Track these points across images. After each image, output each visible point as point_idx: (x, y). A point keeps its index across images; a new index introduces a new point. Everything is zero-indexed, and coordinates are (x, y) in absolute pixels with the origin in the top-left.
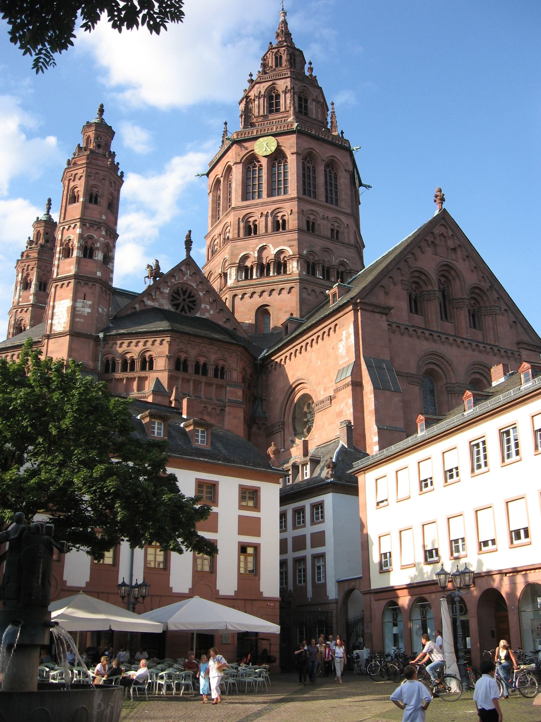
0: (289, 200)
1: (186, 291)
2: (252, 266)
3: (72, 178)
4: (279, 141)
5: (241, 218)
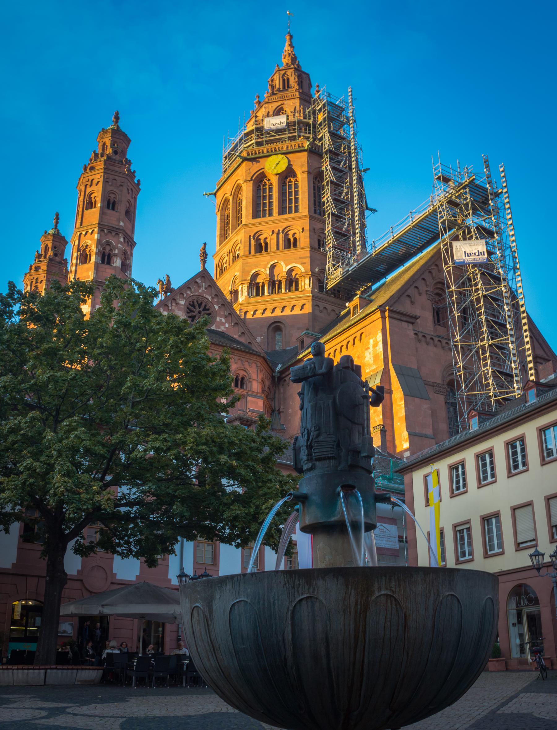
0: (302, 218)
1: (201, 303)
2: (263, 283)
3: (89, 183)
4: (291, 159)
5: (252, 235)
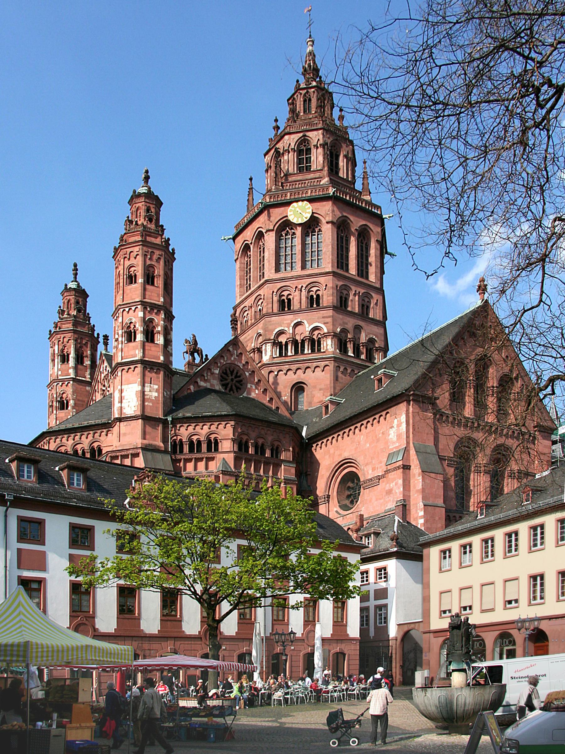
1: (233, 370)
